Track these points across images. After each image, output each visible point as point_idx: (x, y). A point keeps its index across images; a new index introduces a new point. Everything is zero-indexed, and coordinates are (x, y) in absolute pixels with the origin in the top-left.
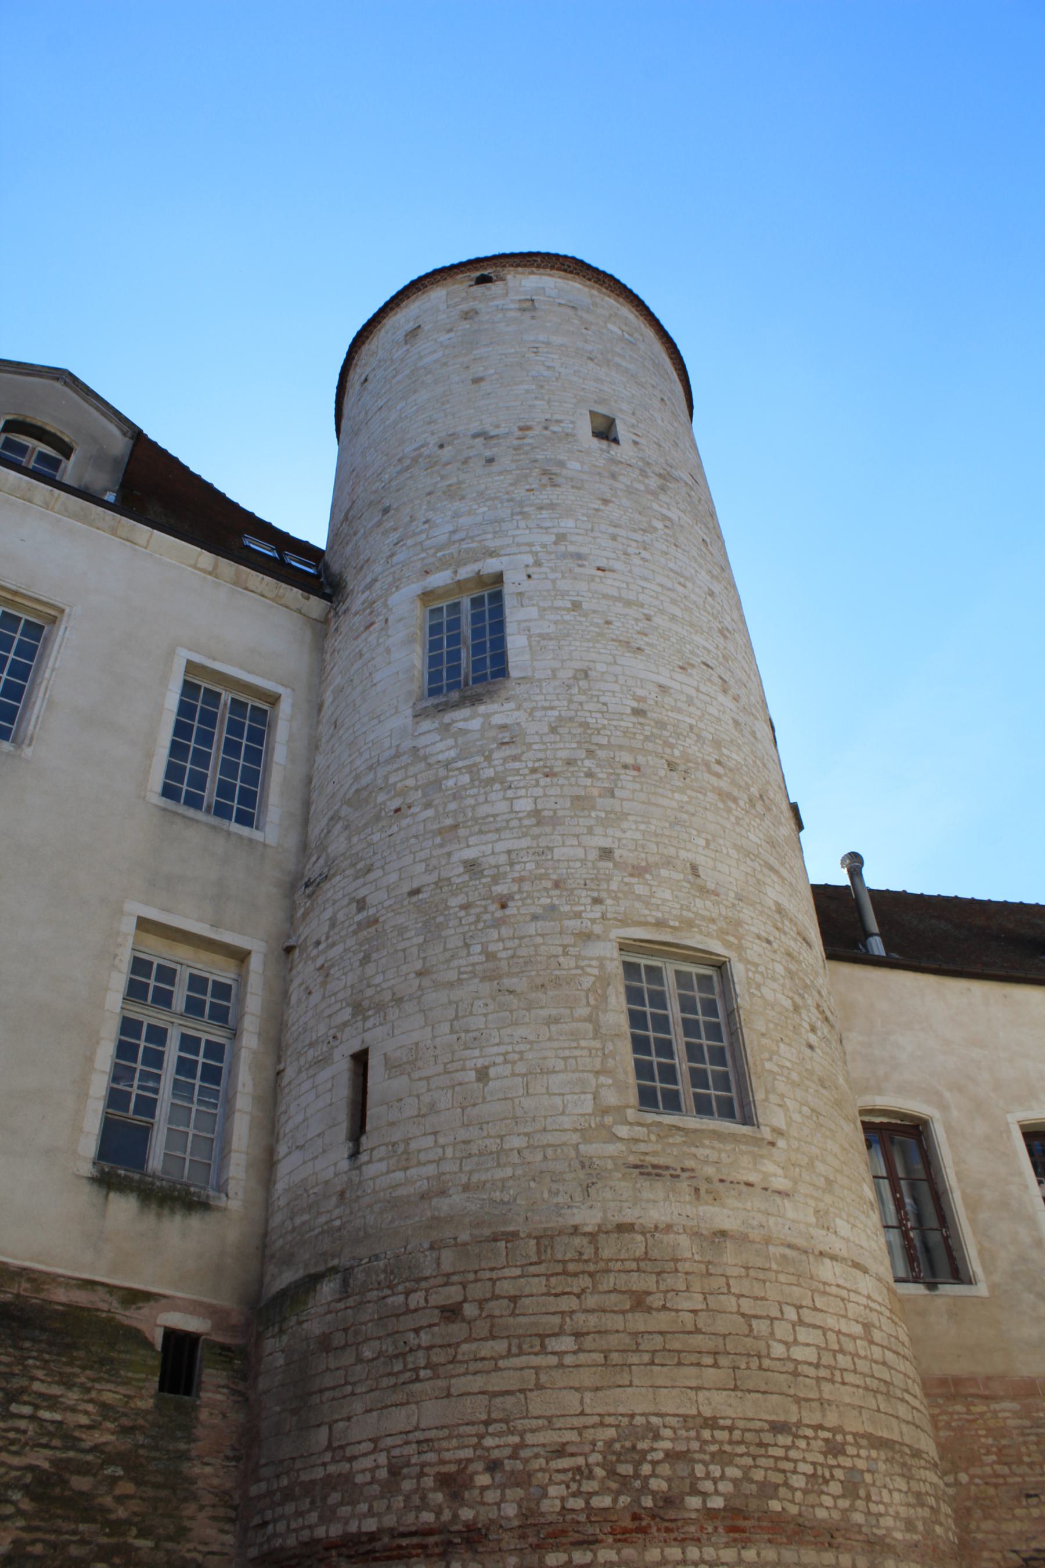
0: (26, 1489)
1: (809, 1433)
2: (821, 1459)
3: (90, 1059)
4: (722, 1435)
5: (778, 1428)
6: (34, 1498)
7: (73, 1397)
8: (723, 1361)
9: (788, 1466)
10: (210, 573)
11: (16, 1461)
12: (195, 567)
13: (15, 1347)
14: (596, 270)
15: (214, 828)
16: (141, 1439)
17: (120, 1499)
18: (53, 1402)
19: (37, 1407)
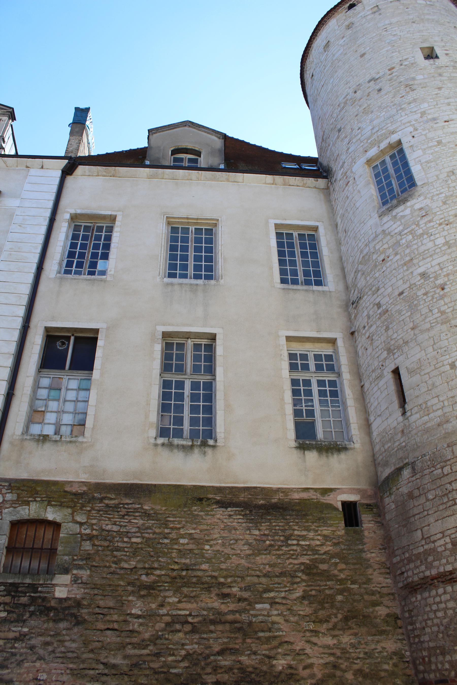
0: (302, 571)
3: (282, 399)
6: (307, 574)
7: (311, 534)
10: (273, 184)
11: (296, 562)
12: (265, 183)
13: (284, 519)
15: (306, 291)
16: (343, 547)
17: (340, 571)
18: (304, 538)
19: (298, 540)
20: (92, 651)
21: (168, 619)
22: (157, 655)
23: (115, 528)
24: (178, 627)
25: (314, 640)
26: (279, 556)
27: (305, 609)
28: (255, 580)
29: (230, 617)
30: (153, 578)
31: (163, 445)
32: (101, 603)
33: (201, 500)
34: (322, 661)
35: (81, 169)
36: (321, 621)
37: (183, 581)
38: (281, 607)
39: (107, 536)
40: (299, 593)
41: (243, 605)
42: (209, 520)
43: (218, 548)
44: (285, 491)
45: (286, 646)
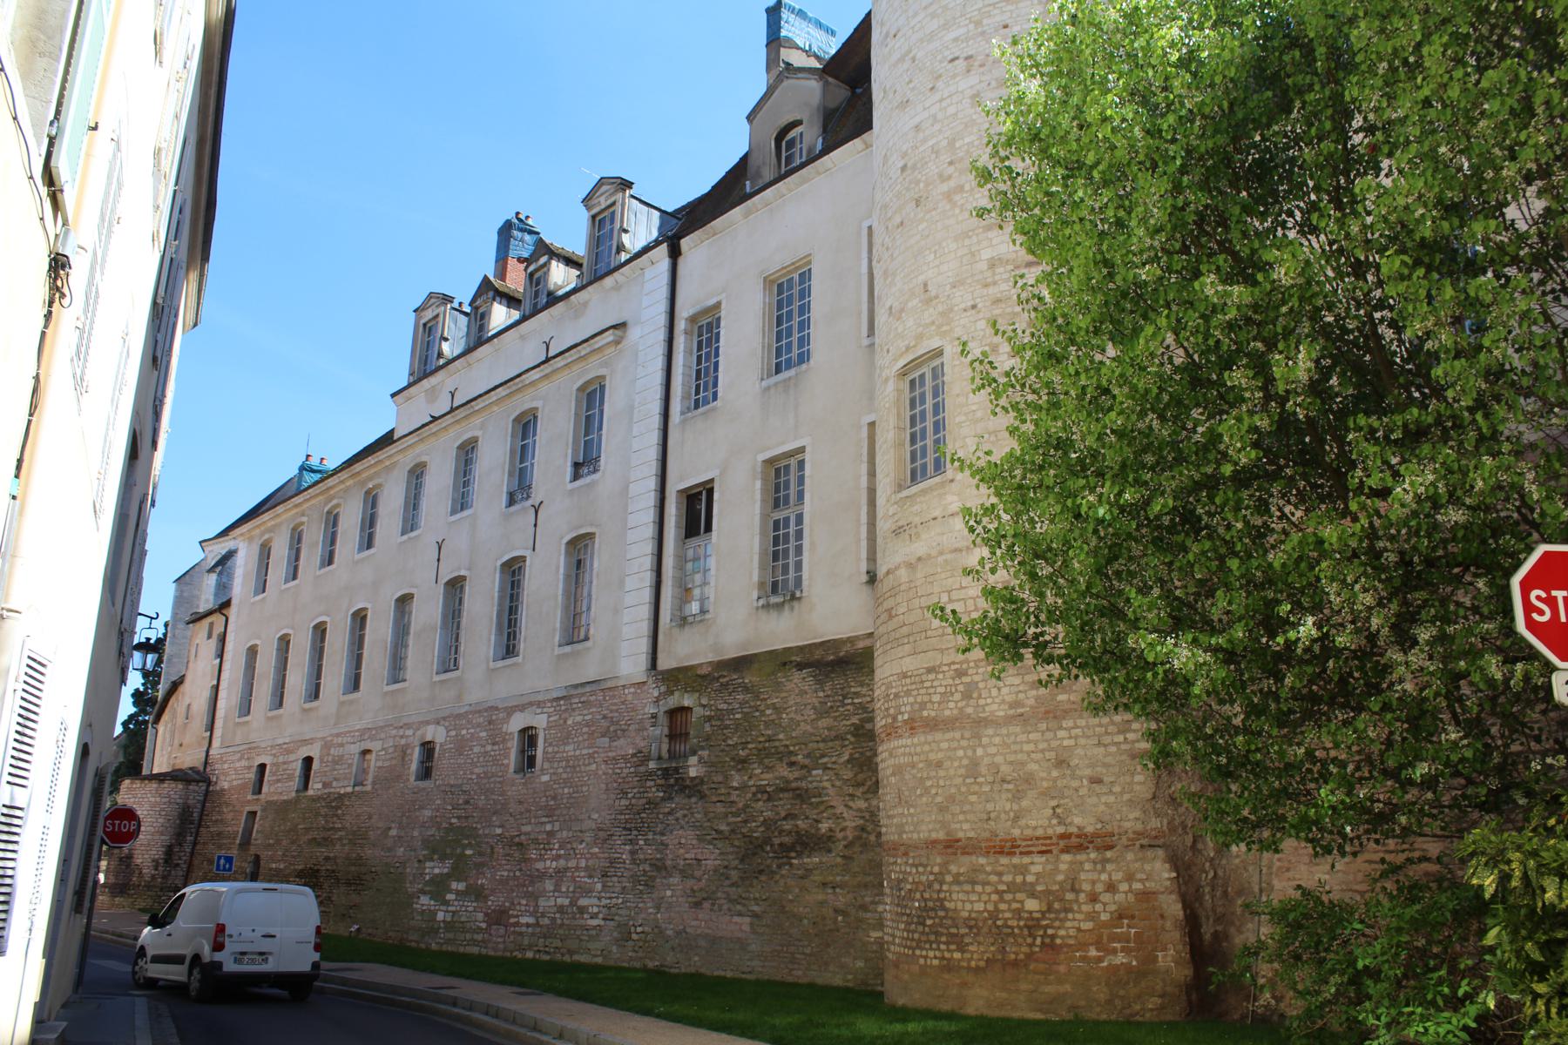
3: (858, 520)
5: (930, 670)
22: (745, 822)
26: (835, 718)
27: (848, 774)
29: (794, 785)
33: (785, 664)
35: (685, 243)
36: (859, 785)
37: (768, 753)
39: (720, 715)
40: (846, 757)
42: (789, 686)
45: (830, 811)
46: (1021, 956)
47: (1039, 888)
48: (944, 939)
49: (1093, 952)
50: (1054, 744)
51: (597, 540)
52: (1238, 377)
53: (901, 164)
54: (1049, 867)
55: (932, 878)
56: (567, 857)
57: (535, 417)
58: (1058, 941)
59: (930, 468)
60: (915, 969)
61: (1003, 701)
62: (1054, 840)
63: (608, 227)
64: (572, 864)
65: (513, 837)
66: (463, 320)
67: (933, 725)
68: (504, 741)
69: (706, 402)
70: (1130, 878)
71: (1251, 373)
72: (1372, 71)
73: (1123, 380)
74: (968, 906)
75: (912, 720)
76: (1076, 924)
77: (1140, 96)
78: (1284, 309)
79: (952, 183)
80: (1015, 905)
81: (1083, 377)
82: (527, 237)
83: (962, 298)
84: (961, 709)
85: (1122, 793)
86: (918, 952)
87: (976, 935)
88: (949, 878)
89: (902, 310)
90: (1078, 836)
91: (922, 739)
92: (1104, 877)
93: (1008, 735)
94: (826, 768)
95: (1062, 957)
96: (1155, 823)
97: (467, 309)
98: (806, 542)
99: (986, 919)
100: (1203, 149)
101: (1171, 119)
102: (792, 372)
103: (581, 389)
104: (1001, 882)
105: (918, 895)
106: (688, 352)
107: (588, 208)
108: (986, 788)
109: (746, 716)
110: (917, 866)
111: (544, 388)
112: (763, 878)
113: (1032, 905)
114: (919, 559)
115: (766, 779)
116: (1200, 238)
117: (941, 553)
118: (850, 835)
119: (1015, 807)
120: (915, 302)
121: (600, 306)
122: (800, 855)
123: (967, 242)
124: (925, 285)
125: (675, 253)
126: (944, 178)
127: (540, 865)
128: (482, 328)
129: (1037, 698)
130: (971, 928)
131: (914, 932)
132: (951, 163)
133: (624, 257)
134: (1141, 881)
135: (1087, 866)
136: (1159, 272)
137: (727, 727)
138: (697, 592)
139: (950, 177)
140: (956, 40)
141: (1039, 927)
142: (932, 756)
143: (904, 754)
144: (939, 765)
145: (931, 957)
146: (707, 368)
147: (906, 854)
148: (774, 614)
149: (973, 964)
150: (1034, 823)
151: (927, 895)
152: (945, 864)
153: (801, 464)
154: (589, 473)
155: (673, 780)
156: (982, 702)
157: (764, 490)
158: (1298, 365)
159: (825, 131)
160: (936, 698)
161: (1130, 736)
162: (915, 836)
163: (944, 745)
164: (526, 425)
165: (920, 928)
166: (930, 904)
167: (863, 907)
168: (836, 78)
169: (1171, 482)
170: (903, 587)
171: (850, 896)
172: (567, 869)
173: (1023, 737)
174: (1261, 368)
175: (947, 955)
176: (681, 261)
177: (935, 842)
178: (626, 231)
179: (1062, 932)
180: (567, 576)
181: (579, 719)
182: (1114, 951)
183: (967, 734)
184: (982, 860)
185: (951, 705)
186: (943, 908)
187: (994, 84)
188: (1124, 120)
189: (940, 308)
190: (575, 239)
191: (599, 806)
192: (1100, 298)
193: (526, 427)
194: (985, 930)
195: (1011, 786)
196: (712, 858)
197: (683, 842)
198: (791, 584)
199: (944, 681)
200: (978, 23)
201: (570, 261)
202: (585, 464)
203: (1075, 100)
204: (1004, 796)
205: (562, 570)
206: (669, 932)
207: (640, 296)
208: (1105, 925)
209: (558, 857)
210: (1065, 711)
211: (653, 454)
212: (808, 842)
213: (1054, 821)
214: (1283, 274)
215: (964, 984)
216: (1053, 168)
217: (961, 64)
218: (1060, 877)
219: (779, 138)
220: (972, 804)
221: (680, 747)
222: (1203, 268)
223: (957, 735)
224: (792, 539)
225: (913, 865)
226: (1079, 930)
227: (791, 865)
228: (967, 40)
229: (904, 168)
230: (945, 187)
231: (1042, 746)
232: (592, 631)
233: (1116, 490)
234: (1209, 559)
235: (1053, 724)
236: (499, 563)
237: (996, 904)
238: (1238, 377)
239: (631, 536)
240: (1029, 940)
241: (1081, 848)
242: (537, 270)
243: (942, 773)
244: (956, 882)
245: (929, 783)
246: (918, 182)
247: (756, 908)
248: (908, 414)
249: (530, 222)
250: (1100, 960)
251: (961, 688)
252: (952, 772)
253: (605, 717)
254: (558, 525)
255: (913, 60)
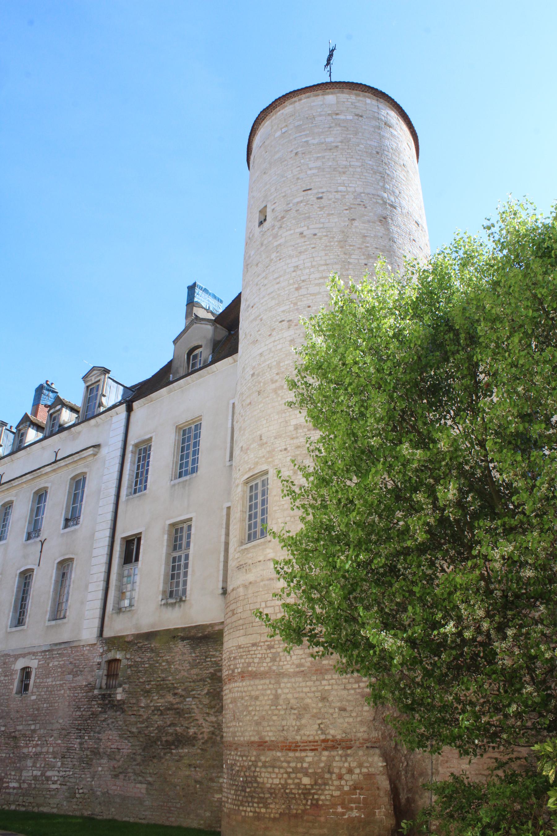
0: (209, 678)
1: (262, 644)
2: (265, 651)
3: (219, 559)
4: (241, 650)
5: (254, 645)
6: (211, 679)
8: (244, 627)
9: (254, 656)
11: (208, 672)
14: (270, 105)
18: (214, 656)
20: (126, 726)
21: (153, 708)
22: (147, 727)
23: (139, 660)
24: (156, 712)
25: (207, 718)
26: (201, 669)
27: (206, 701)
28: (188, 684)
29: (176, 706)
30: (150, 686)
31: (164, 604)
32: (131, 701)
33: (174, 637)
34: (208, 730)
35: (135, 405)
36: (212, 707)
38: (197, 700)
39: (136, 665)
41: (181, 699)
42: (176, 650)
43: (177, 666)
44: (212, 625)
45: (195, 722)
46: (299, 811)
47: (310, 771)
48: (256, 800)
49: (340, 810)
50: (320, 688)
51: (75, 562)
52: (419, 497)
53: (251, 373)
54: (316, 759)
55: (250, 763)
56: (42, 746)
57: (46, 492)
58: (320, 803)
59: (259, 534)
60: (239, 818)
61: (293, 664)
62: (319, 743)
63: (95, 393)
64: (44, 750)
65: (11, 733)
66: (11, 436)
67: (254, 675)
68: (12, 674)
69: (140, 491)
70: (360, 766)
71: (426, 495)
72: (487, 347)
73: (360, 496)
74: (270, 781)
75: (243, 672)
76: (330, 792)
77: (375, 351)
78: (443, 463)
79: (277, 384)
80: (297, 781)
81: (340, 493)
82: (51, 394)
83: (280, 444)
84: (270, 667)
85: (356, 717)
86: (241, 808)
87: (274, 798)
88: (260, 764)
89: (248, 449)
90: (332, 741)
91: (248, 683)
92: (346, 765)
93: (295, 683)
94: (194, 697)
95: (322, 812)
96: (374, 734)
97: (14, 430)
98: (190, 570)
99: (280, 789)
100: (404, 379)
101: (389, 364)
102: (188, 477)
103: (73, 479)
104: (290, 767)
105: (242, 774)
106: (133, 463)
107: (85, 382)
108: (282, 712)
109: (151, 666)
110: (242, 756)
111: (53, 477)
112: (155, 761)
113: (306, 781)
114: (250, 583)
115: (161, 702)
116: (402, 425)
117: (262, 580)
118: (206, 736)
119: (298, 724)
120: (255, 445)
121: (87, 435)
122: (177, 747)
123: (284, 415)
124: (261, 436)
125: (130, 409)
126: (273, 381)
127: (25, 750)
128: (21, 441)
129: (311, 662)
130: (271, 794)
131: (239, 795)
132: (277, 374)
133: (102, 409)
134: (366, 767)
135: (337, 758)
136: (380, 441)
137: (140, 671)
138: (128, 594)
139: (276, 381)
140: (283, 311)
141: (310, 793)
142: (253, 693)
143: (238, 692)
144: (257, 698)
145: (249, 811)
146: (142, 472)
147: (236, 749)
148: (170, 609)
149: (272, 815)
150: (308, 733)
151: (247, 774)
152: (258, 756)
153: (190, 527)
154: (74, 525)
155: (107, 701)
156: (281, 663)
157: (169, 540)
158: (449, 492)
159: (213, 352)
160: (256, 660)
161: (362, 685)
162: (242, 739)
163: (260, 687)
164: (41, 496)
165: (243, 794)
166: (249, 779)
167: (212, 780)
168: (221, 325)
169: (385, 550)
170: (241, 598)
171: (204, 773)
172: (41, 753)
173: (303, 684)
174: (432, 492)
175: (257, 810)
176: (133, 414)
177: (253, 743)
178: (104, 396)
179: (323, 797)
180: (56, 582)
181: (56, 663)
182: (352, 809)
183: (273, 681)
184: (279, 754)
185: (265, 664)
186: (256, 781)
187: (302, 335)
188: (365, 363)
189: (268, 449)
190: (76, 398)
191: (63, 715)
192: (350, 453)
193: (40, 497)
194: (279, 795)
195: (296, 712)
196: (126, 748)
197: (110, 738)
198: (180, 592)
199: (260, 651)
200: (295, 304)
201: (73, 409)
202: (71, 519)
203: (341, 350)
204: (292, 717)
205: (54, 578)
206: (99, 793)
207: (109, 432)
208: (347, 793)
209: (37, 745)
210: (327, 670)
211: (109, 517)
212: (182, 740)
213: (319, 732)
214: (443, 446)
215: (267, 829)
216: (328, 386)
217: (285, 324)
218: (322, 765)
219: (189, 354)
220: (274, 721)
221: (113, 682)
222: (404, 440)
223: (267, 681)
224: (182, 568)
225: (241, 756)
226: (332, 796)
227: (172, 753)
228: (289, 312)
229: (253, 375)
230: (273, 386)
231: (313, 689)
232: (68, 614)
233: (355, 554)
234: (404, 590)
235: (320, 677)
236: (19, 572)
237: (286, 779)
238: (419, 497)
239: (94, 561)
240: (304, 802)
241: (334, 748)
242: (54, 413)
243: (258, 703)
244: (264, 766)
245: (250, 708)
246: (260, 383)
247: (150, 779)
248: (248, 504)
249: (53, 386)
250: (343, 814)
251: (270, 655)
252: (264, 702)
253: (71, 663)
254: (54, 552)
255: (261, 320)
